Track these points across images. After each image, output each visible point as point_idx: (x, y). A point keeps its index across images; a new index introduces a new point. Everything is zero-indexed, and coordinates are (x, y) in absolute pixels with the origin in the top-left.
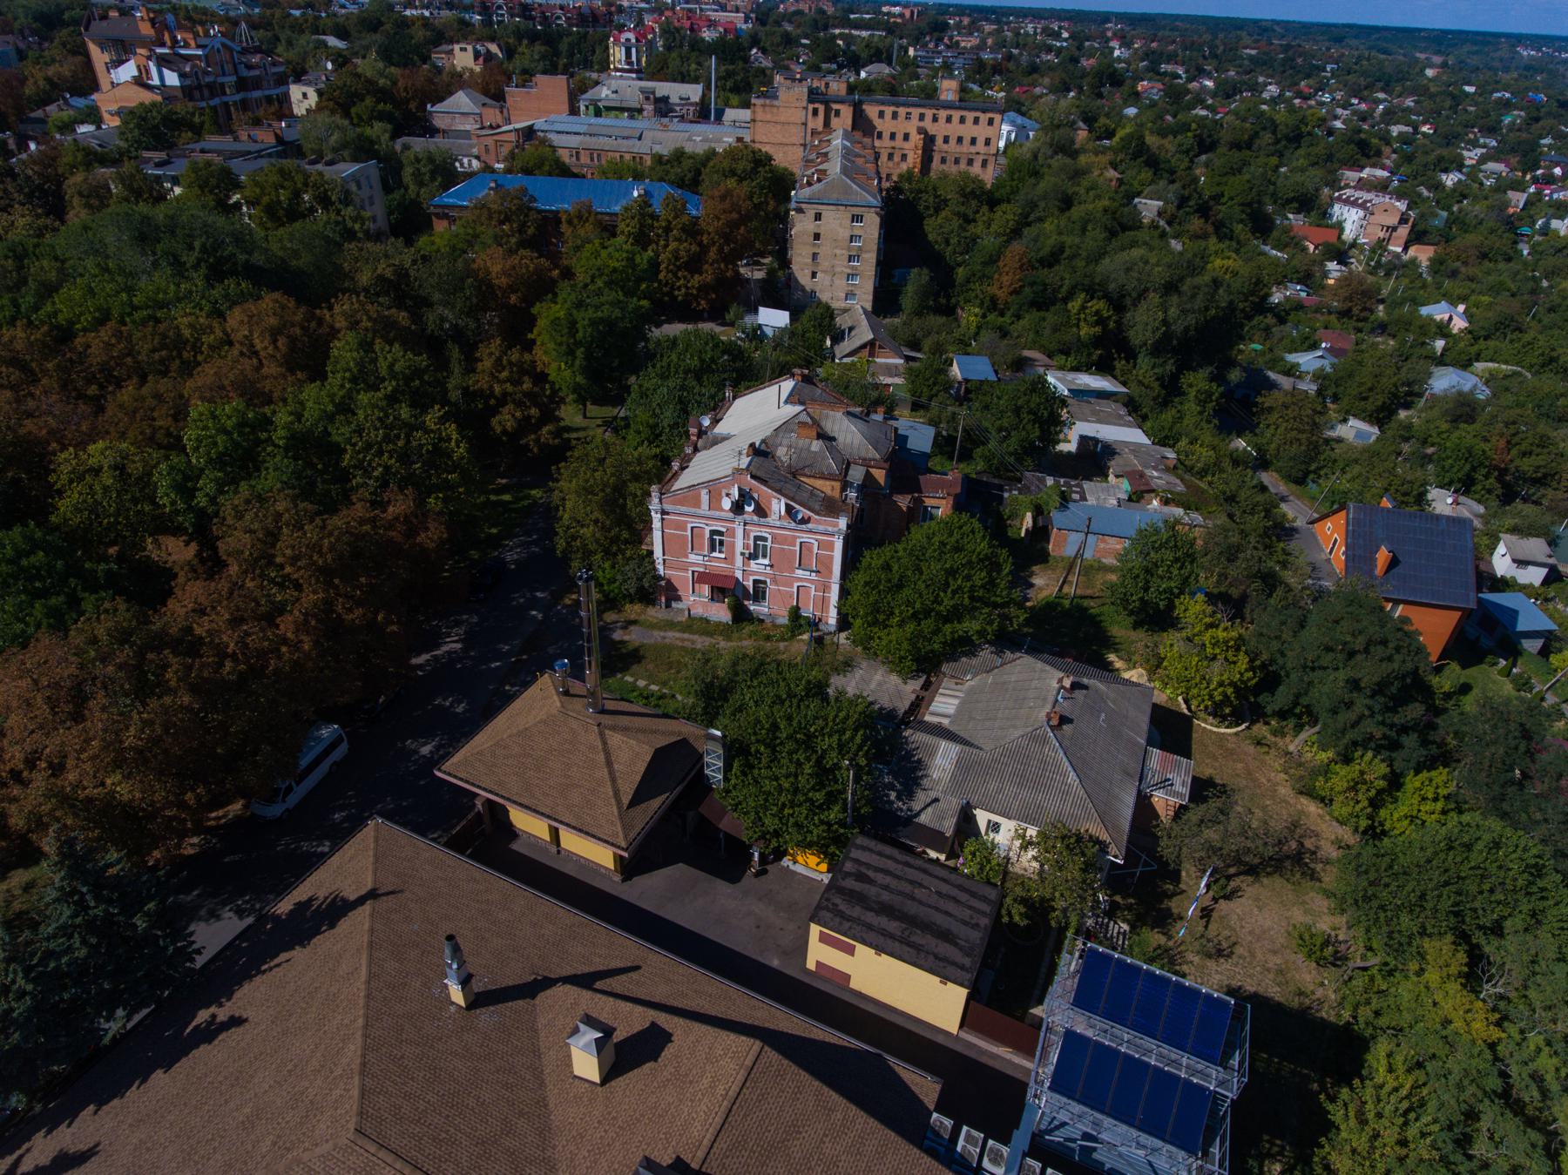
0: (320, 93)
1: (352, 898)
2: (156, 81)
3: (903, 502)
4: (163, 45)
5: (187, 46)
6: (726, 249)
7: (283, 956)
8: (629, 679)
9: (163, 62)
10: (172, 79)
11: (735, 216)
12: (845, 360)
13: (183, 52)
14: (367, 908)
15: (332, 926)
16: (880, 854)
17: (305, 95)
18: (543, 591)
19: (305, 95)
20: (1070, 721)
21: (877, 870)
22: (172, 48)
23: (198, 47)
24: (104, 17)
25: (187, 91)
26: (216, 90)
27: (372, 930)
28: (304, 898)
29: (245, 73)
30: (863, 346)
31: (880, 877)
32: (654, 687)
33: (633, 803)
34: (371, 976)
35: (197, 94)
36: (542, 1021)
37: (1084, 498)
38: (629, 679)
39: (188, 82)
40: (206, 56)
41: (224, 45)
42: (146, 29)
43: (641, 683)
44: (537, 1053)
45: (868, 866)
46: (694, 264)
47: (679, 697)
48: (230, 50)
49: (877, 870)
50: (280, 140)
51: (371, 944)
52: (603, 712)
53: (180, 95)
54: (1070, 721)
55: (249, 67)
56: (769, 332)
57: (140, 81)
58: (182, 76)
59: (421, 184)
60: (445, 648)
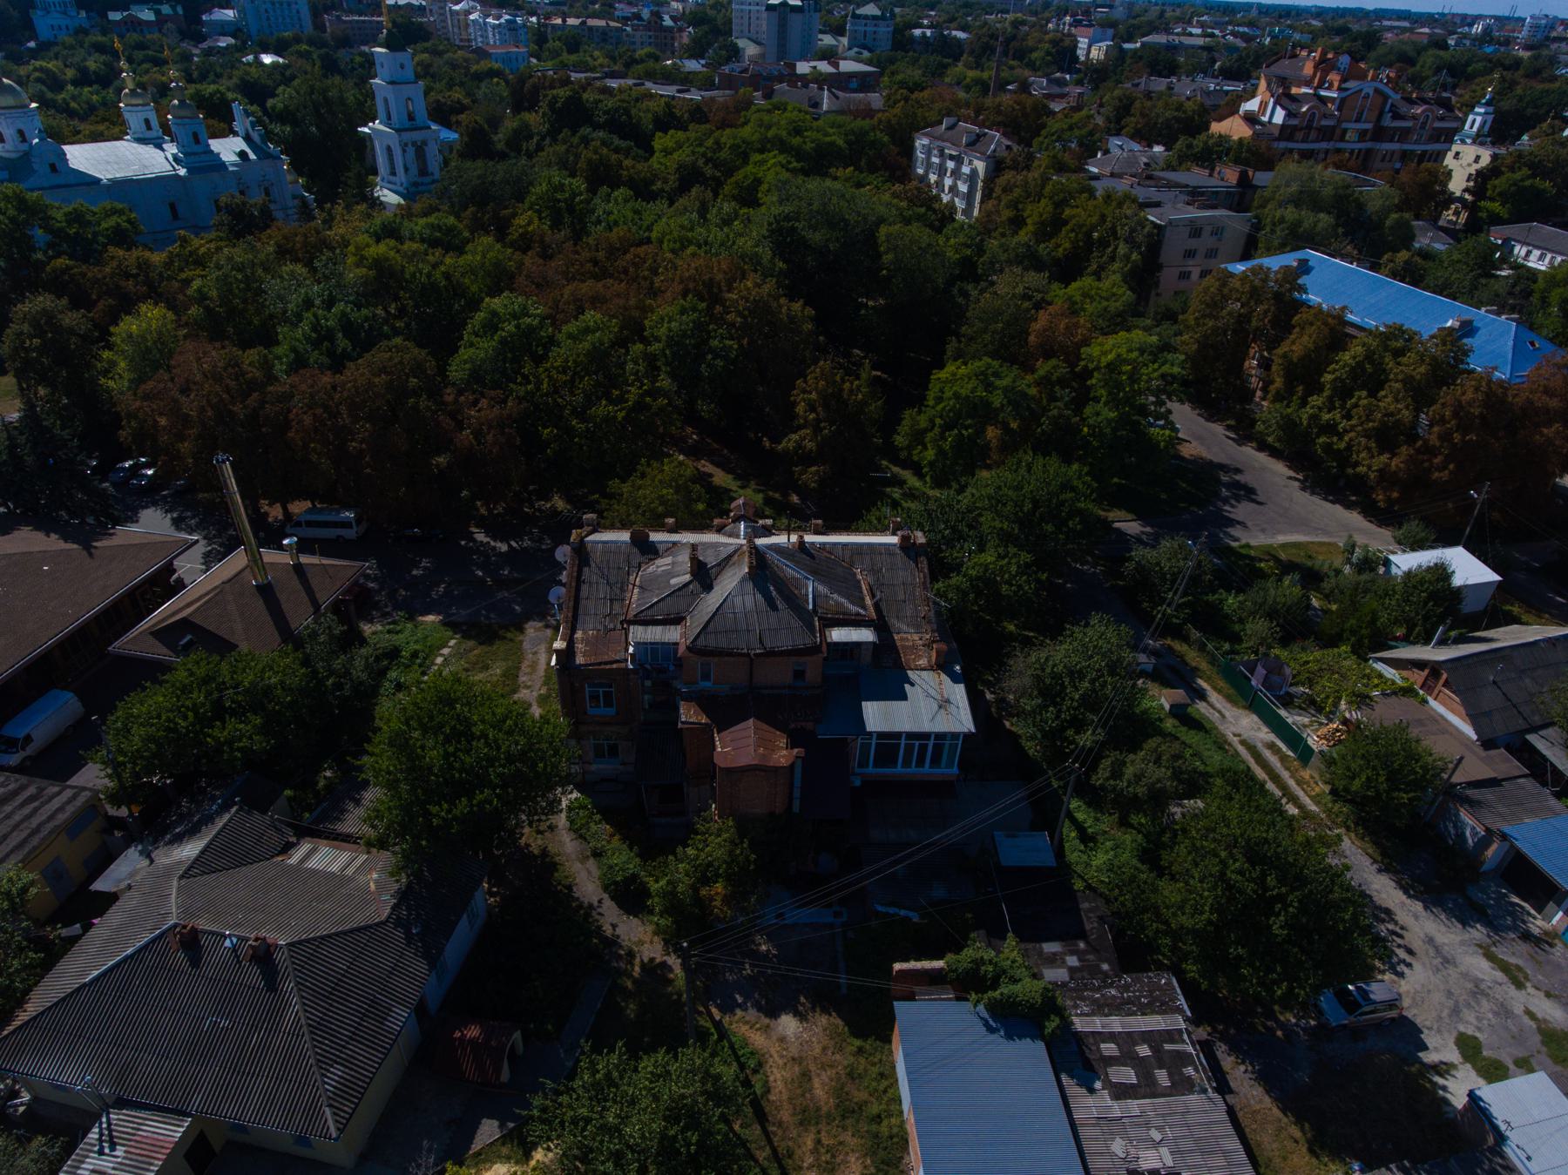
0: (1494, 157)
2: (1265, 119)
3: (689, 714)
4: (1308, 84)
5: (1328, 89)
6: (1457, 437)
9: (1285, 99)
10: (1279, 117)
11: (1554, 403)
12: (1379, 666)
13: (1323, 93)
16: (61, 809)
17: (1477, 159)
19: (1477, 159)
20: (195, 962)
21: (36, 810)
22: (1316, 89)
23: (1340, 89)
24: (1294, 56)
25: (1286, 132)
26: (1327, 134)
29: (1387, 122)
30: (1419, 665)
31: (27, 810)
32: (439, 660)
33: (152, 633)
35: (1299, 135)
37: (1121, 1092)
39: (1294, 122)
40: (1342, 104)
41: (1377, 91)
42: (1308, 69)
43: (446, 651)
45: (43, 804)
46: (1388, 437)
48: (1386, 97)
49: (36, 810)
50: (1244, 181)
52: (266, 591)
53: (1276, 133)
54: (195, 962)
55: (1397, 116)
56: (1394, 570)
57: (1251, 119)
58: (1290, 115)
59: (1268, 250)
60: (499, 545)
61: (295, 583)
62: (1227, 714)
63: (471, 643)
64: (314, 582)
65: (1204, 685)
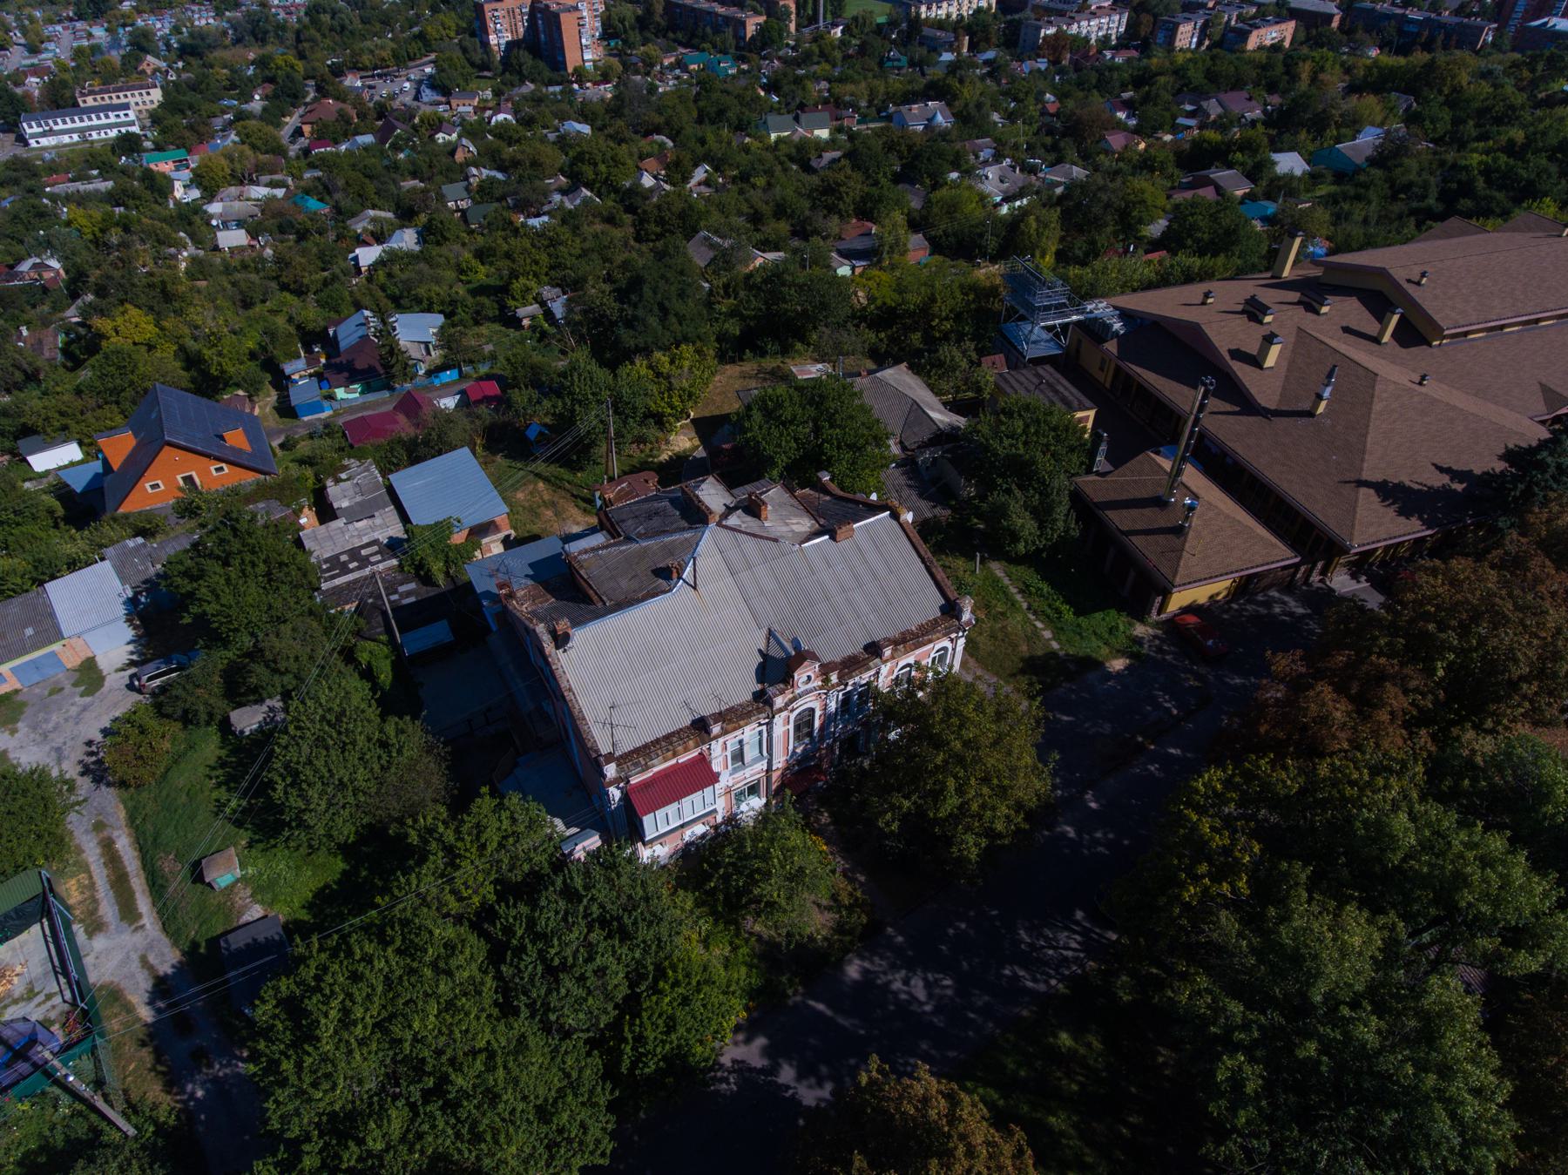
1: (1372, 491)
7: (1416, 487)
8: (1055, 645)
14: (1366, 476)
15: (1385, 482)
18: (1064, 835)
27: (1363, 460)
28: (1402, 519)
32: (1039, 625)
34: (1365, 435)
36: (1277, 398)
38: (1055, 645)
43: (1047, 634)
44: (1284, 388)
47: (1025, 605)
51: (1364, 452)
61: (1163, 524)
62: (135, 965)
63: (1040, 653)
64: (1161, 538)
65: (146, 1014)
